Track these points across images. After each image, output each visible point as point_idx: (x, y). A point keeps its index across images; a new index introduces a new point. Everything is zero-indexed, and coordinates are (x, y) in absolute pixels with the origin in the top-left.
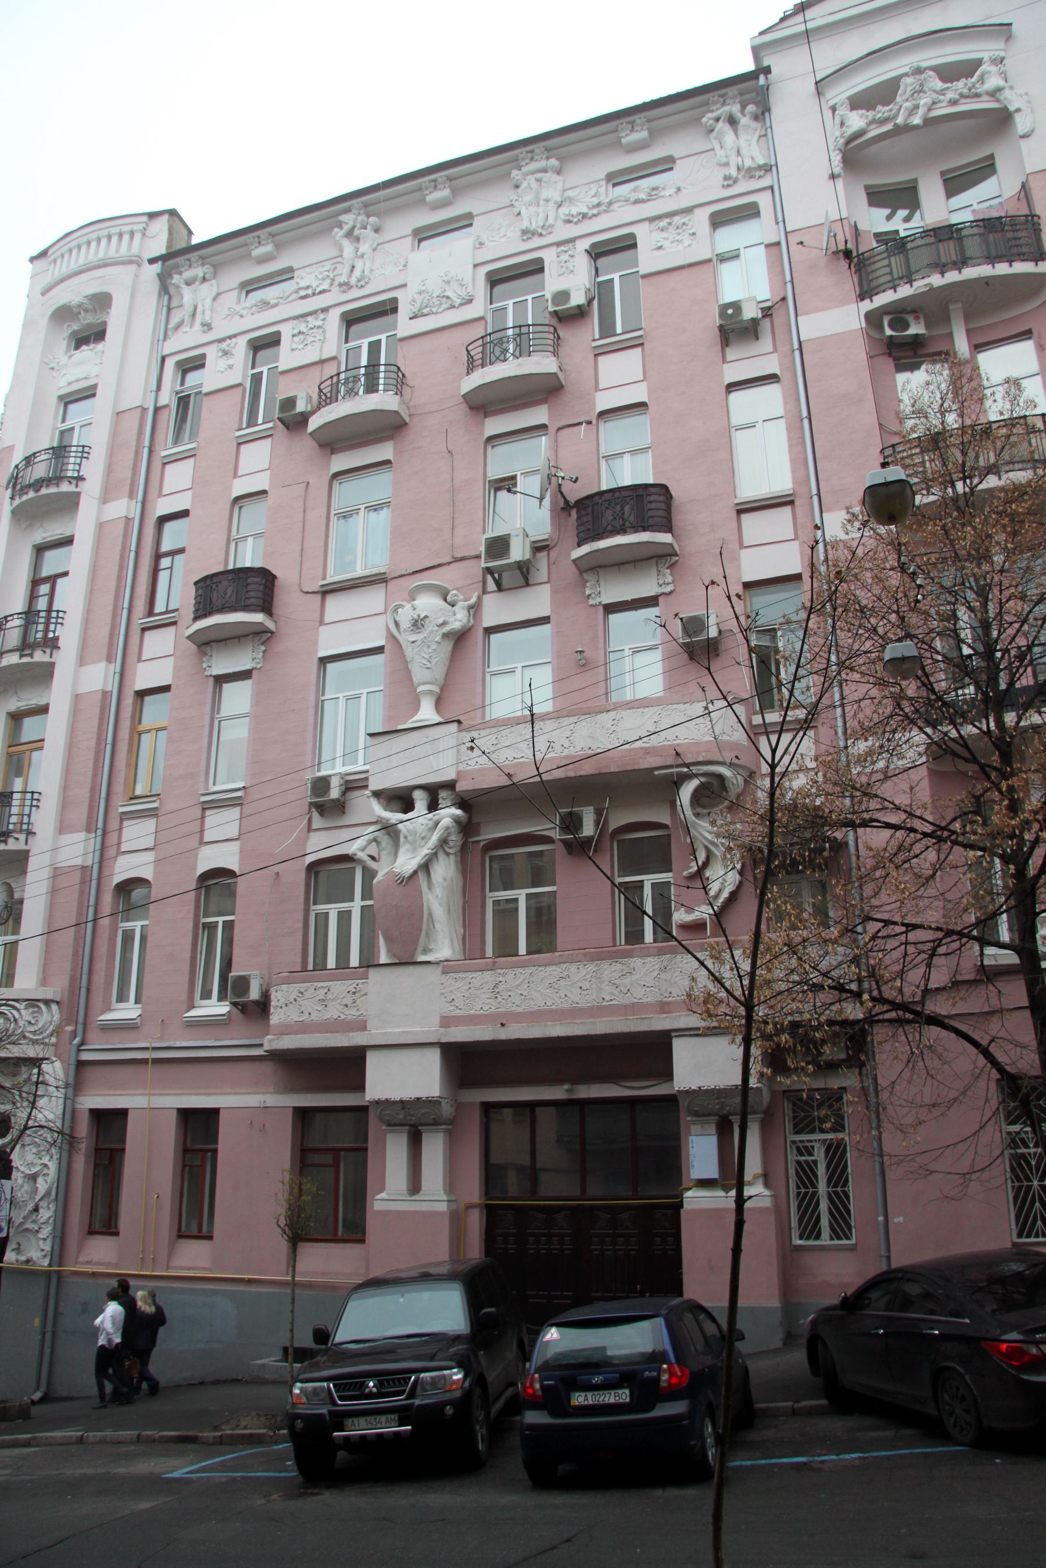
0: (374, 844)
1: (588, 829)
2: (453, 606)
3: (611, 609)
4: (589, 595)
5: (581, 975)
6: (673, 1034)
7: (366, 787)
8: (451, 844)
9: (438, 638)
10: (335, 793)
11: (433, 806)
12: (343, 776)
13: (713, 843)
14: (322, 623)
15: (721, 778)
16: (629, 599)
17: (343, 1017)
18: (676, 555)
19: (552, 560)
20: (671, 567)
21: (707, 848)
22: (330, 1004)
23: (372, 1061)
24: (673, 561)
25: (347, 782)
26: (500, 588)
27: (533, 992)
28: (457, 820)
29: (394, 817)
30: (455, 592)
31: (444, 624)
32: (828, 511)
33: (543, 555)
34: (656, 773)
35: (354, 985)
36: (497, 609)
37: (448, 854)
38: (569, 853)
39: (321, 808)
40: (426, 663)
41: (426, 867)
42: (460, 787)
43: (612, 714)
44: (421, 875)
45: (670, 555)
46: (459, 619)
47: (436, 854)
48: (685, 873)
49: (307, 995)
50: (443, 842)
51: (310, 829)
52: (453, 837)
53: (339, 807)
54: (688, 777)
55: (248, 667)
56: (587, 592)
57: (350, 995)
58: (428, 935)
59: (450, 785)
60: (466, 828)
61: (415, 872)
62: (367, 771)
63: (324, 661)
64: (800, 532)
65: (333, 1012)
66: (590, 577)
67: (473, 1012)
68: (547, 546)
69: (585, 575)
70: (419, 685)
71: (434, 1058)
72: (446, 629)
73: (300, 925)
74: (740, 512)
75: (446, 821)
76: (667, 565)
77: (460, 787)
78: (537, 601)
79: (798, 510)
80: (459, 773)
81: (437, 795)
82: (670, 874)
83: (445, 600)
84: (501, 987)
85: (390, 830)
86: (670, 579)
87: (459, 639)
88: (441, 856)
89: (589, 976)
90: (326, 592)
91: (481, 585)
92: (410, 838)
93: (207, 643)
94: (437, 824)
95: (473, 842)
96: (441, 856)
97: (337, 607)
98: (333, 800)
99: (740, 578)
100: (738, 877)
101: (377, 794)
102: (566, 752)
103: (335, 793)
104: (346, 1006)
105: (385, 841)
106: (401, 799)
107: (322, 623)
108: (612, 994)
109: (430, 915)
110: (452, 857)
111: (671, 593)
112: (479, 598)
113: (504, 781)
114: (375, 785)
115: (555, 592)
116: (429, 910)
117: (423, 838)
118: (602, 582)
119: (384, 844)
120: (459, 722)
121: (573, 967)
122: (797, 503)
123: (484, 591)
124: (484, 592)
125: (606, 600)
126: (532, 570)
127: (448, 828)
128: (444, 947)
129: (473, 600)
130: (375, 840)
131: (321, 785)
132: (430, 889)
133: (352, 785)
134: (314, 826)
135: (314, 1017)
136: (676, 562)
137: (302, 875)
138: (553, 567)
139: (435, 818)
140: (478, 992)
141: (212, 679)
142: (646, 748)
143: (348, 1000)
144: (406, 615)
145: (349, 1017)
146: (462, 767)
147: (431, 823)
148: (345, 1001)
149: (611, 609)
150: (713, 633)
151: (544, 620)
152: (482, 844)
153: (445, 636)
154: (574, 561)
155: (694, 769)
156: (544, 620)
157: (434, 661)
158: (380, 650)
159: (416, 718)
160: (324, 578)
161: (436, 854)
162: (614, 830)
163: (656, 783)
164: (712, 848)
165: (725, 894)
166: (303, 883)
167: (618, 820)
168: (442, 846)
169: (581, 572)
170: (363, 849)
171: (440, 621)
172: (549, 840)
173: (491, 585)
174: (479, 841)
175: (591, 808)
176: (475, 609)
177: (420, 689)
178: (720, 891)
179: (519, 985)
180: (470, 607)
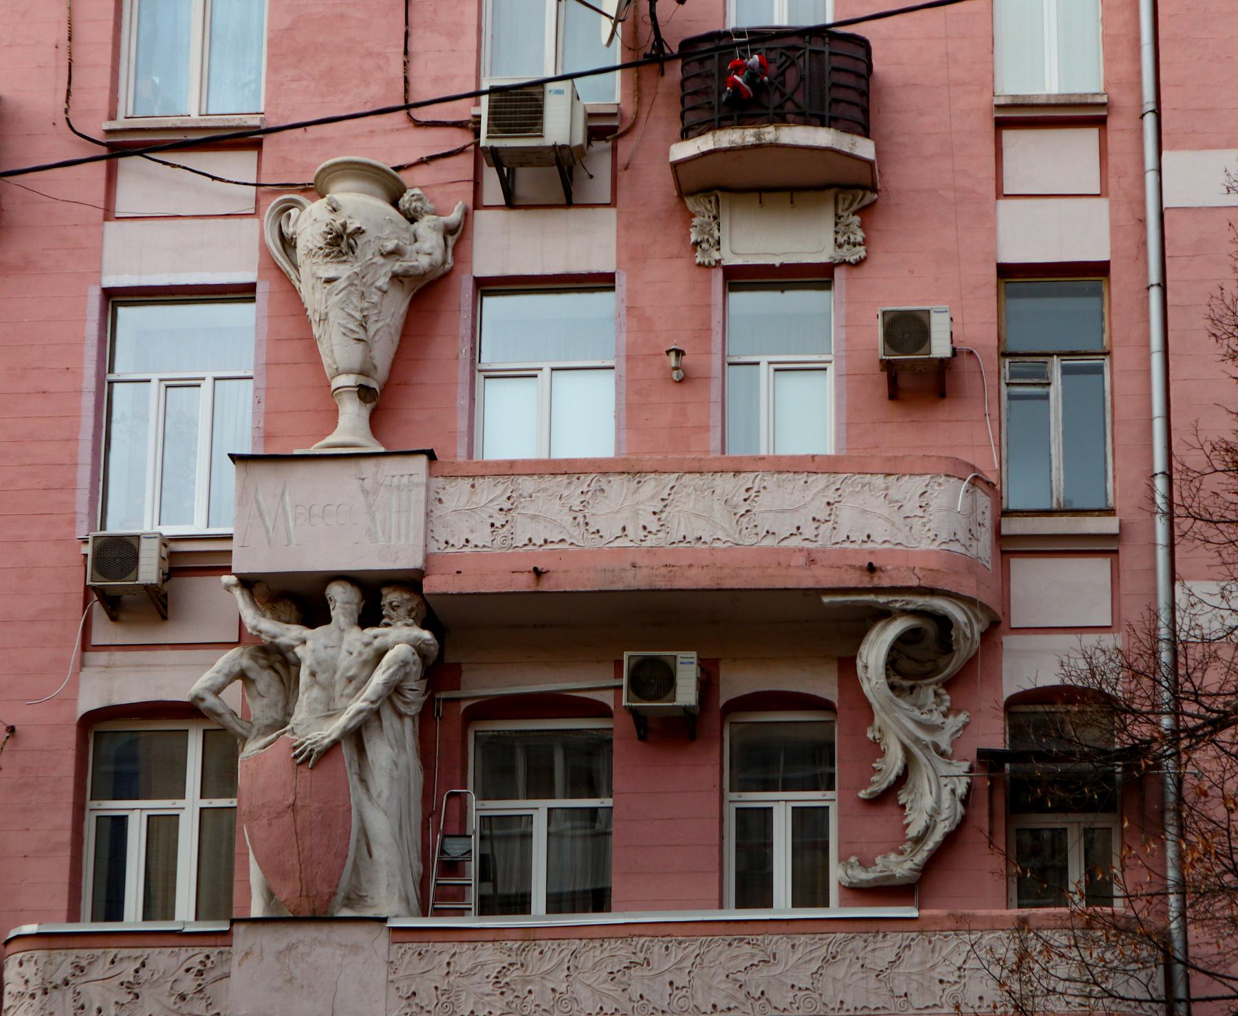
0: (239, 683)
1: (686, 693)
2: (412, 220)
3: (741, 278)
4: (697, 244)
5: (672, 960)
7: (227, 570)
8: (410, 696)
9: (383, 281)
10: (149, 570)
11: (370, 616)
12: (166, 541)
13: (917, 740)
14: (109, 214)
15: (944, 622)
16: (777, 262)
18: (874, 190)
19: (622, 159)
20: (865, 212)
21: (906, 749)
22: (145, 991)
24: (867, 201)
25: (173, 555)
26: (511, 202)
27: (578, 986)
28: (419, 649)
29: (289, 633)
30: (417, 191)
31: (396, 253)
32: (1172, 148)
33: (601, 146)
34: (826, 599)
35: (201, 957)
36: (504, 244)
37: (401, 716)
38: (642, 738)
40: (345, 327)
41: (356, 736)
42: (431, 585)
43: (746, 480)
44: (346, 751)
45: (864, 188)
46: (427, 248)
47: (377, 713)
48: (863, 794)
49: (97, 971)
50: (394, 690)
51: (86, 646)
52: (411, 684)
54: (885, 614)
56: (693, 238)
57: (191, 976)
58: (356, 869)
59: (410, 581)
60: (436, 670)
61: (336, 744)
62: (229, 538)
63: (115, 298)
64: (1112, 182)
66: (701, 209)
68: (615, 128)
69: (689, 202)
70: (338, 373)
72: (398, 266)
73: (66, 836)
74: (1002, 124)
75: (400, 651)
76: (855, 207)
77: (431, 585)
78: (586, 240)
79: (1114, 138)
80: (427, 557)
81: (380, 597)
82: (829, 794)
83: (395, 203)
84: (514, 974)
85: (280, 661)
86: (859, 236)
87: (425, 294)
88: (388, 718)
89: (688, 963)
90: (120, 148)
91: (471, 186)
92: (321, 677)
94: (381, 654)
95: (446, 700)
96: (388, 718)
97: (140, 183)
98: (146, 587)
99: (994, 252)
100: (960, 808)
101: (248, 583)
102: (651, 541)
103: (149, 570)
104: (183, 997)
105: (265, 679)
106: (301, 598)
107: (109, 214)
108: (733, 997)
109: (364, 832)
110: (408, 722)
111: (860, 263)
112: (466, 214)
113: (523, 583)
114: (241, 564)
115: (625, 226)
116: (362, 820)
117: (350, 680)
118: (725, 221)
119: (261, 687)
120: (431, 455)
121: (657, 948)
122: (1112, 123)
123: (477, 204)
124: (477, 204)
125: (731, 260)
126: (579, 174)
127: (405, 664)
128: (389, 894)
129: (455, 216)
130: (243, 675)
131: (117, 553)
132: (363, 781)
133: (189, 562)
134: (96, 639)
136: (874, 203)
137: (70, 738)
138: (624, 177)
139: (377, 643)
140: (464, 981)
142: (809, 552)
144: (311, 223)
146: (433, 548)
147: (368, 653)
148: (181, 988)
149: (741, 278)
150: (940, 347)
151: (602, 282)
152: (464, 705)
153: (396, 278)
154: (676, 166)
155: (899, 602)
156: (602, 282)
157: (372, 328)
158: (243, 293)
159: (330, 439)
160: (112, 117)
161: (377, 713)
162: (728, 703)
163: (819, 619)
164: (916, 750)
165: (937, 836)
166: (71, 753)
167: (739, 681)
168: (389, 698)
169: (683, 193)
170: (217, 691)
171: (390, 245)
172: (600, 710)
173: (493, 190)
174: (459, 700)
175: (694, 654)
176: (457, 235)
177: (335, 384)
178: (928, 830)
179: (549, 972)
180: (449, 231)
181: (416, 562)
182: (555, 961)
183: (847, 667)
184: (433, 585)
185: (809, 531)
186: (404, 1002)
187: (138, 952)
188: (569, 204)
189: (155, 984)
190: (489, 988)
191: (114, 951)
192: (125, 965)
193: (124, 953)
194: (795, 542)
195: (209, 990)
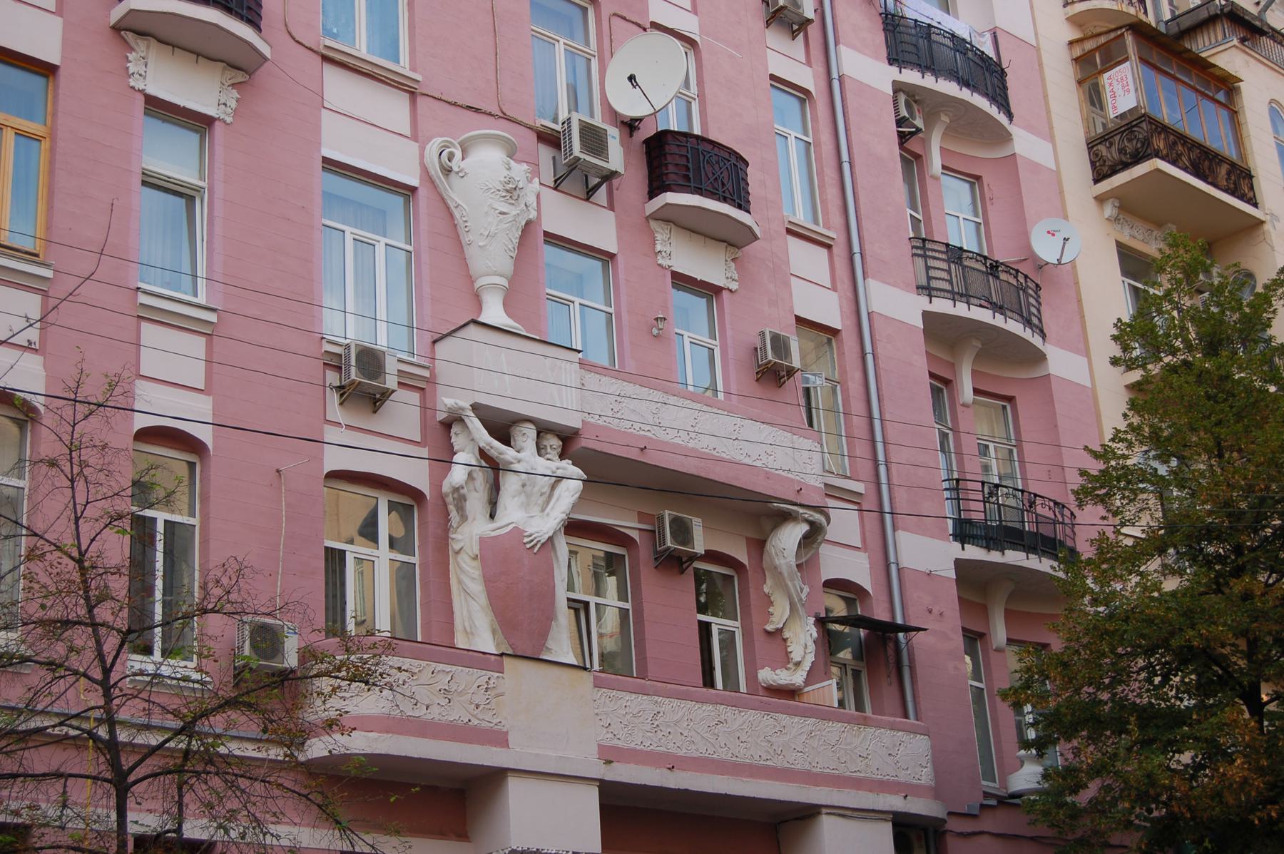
6: (824, 811)
17: (475, 722)
23: (516, 792)
39: (347, 393)
49: (425, 677)
53: (375, 400)
55: (211, 111)
65: (458, 714)
67: (632, 745)
71: (590, 800)
92: (528, 488)
93: (141, 34)
113: (634, 454)
135: (435, 714)
141: (140, 101)
143: (480, 698)
145: (484, 724)
148: (477, 700)
181: (576, 424)
182: (680, 714)
183: (759, 545)
184: (585, 442)
185: (764, 457)
186: (605, 731)
187: (448, 668)
188: (587, 200)
189: (461, 694)
190: (648, 727)
191: (434, 665)
192: (441, 676)
193: (441, 667)
194: (758, 463)
195: (493, 705)
